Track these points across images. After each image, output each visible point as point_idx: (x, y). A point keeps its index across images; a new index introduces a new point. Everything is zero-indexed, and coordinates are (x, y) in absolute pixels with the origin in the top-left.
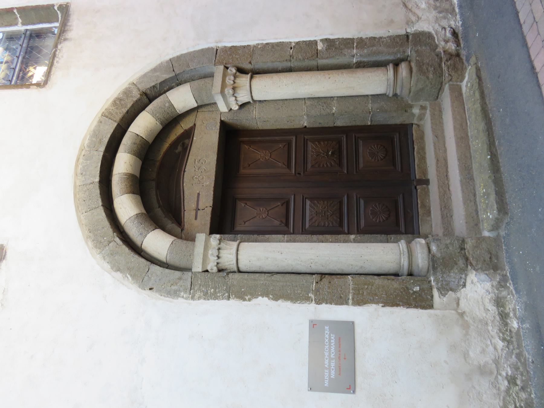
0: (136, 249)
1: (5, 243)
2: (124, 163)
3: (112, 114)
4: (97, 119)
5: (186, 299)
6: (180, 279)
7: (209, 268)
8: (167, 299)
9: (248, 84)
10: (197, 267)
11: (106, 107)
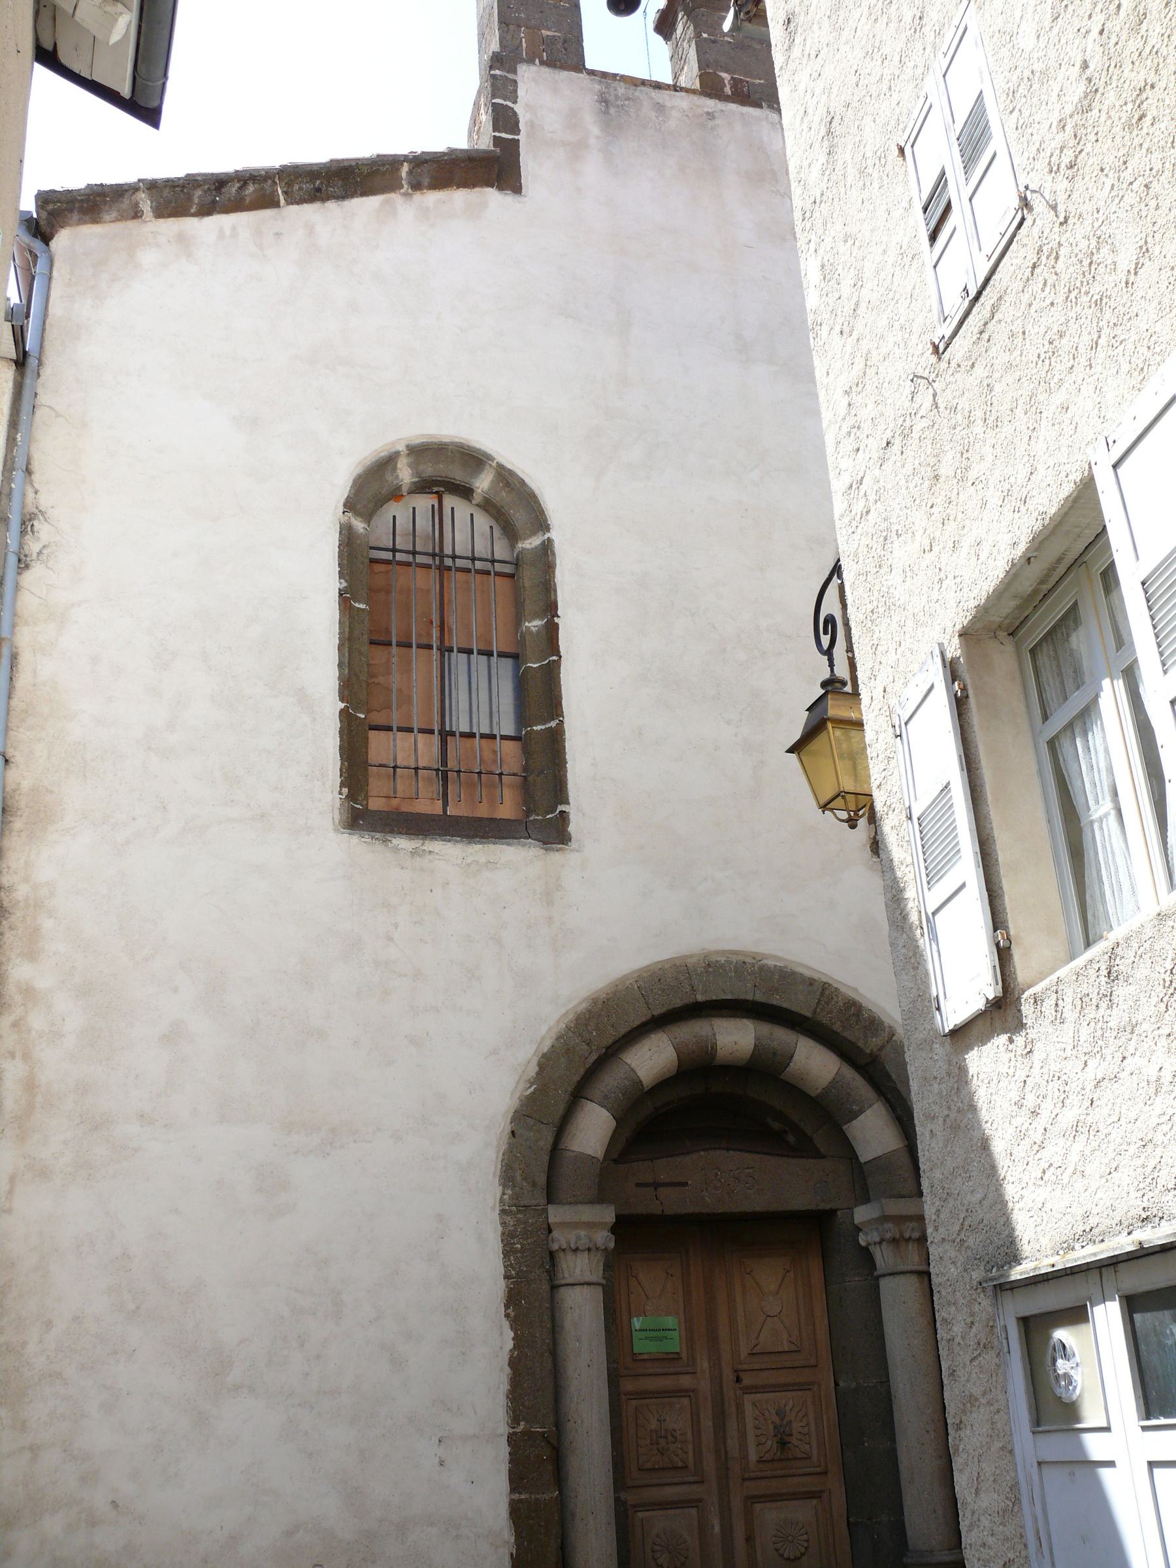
0: (578, 1094)
1: (573, 844)
2: (736, 1038)
3: (827, 1004)
4: (816, 976)
5: (502, 1201)
6: (534, 1184)
7: (556, 1234)
8: (499, 1166)
9: (909, 1268)
10: (555, 1214)
11: (843, 989)
